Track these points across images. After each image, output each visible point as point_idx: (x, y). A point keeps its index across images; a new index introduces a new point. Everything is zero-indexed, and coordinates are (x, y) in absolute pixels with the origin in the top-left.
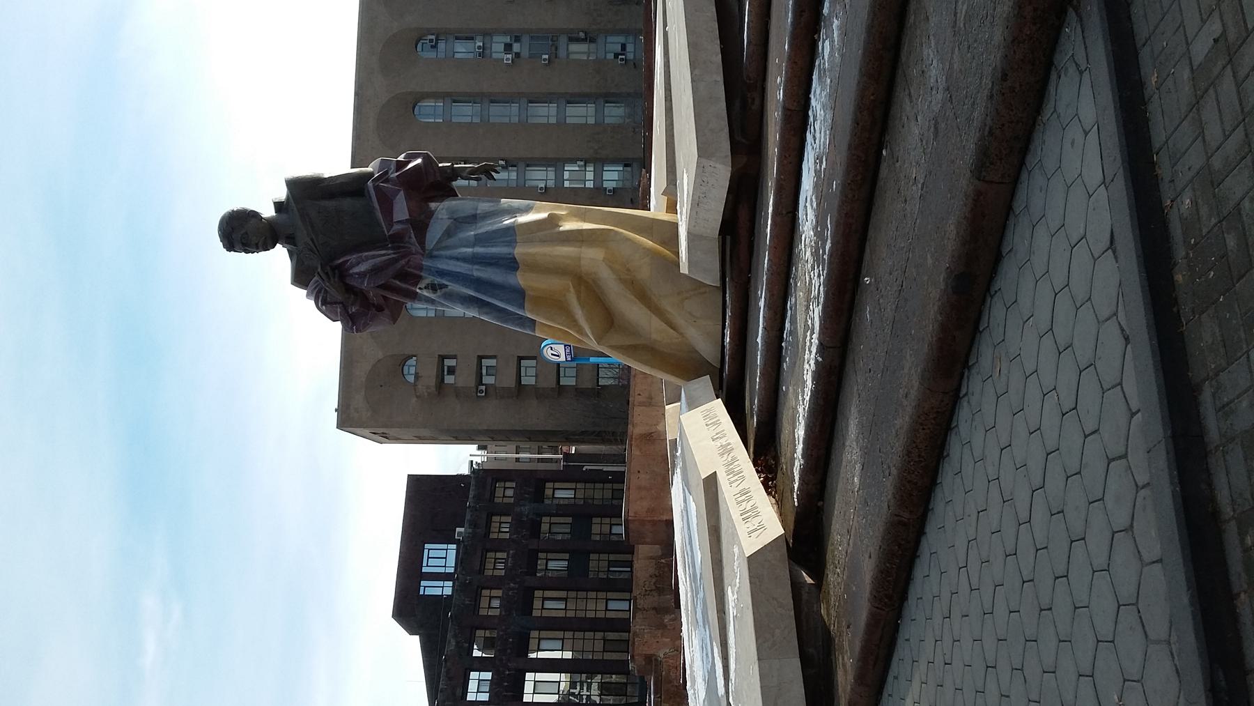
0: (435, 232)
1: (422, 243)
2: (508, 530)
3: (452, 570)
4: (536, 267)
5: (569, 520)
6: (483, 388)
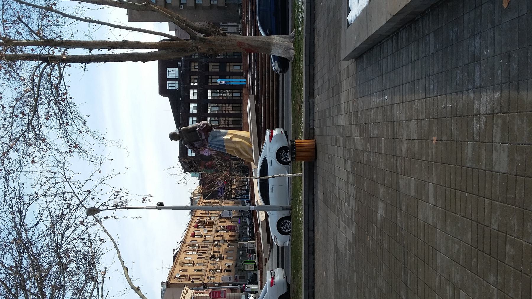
0: (209, 140)
1: (207, 141)
2: (197, 68)
3: (178, 78)
4: (228, 147)
5: (218, 64)
6: (182, 5)
